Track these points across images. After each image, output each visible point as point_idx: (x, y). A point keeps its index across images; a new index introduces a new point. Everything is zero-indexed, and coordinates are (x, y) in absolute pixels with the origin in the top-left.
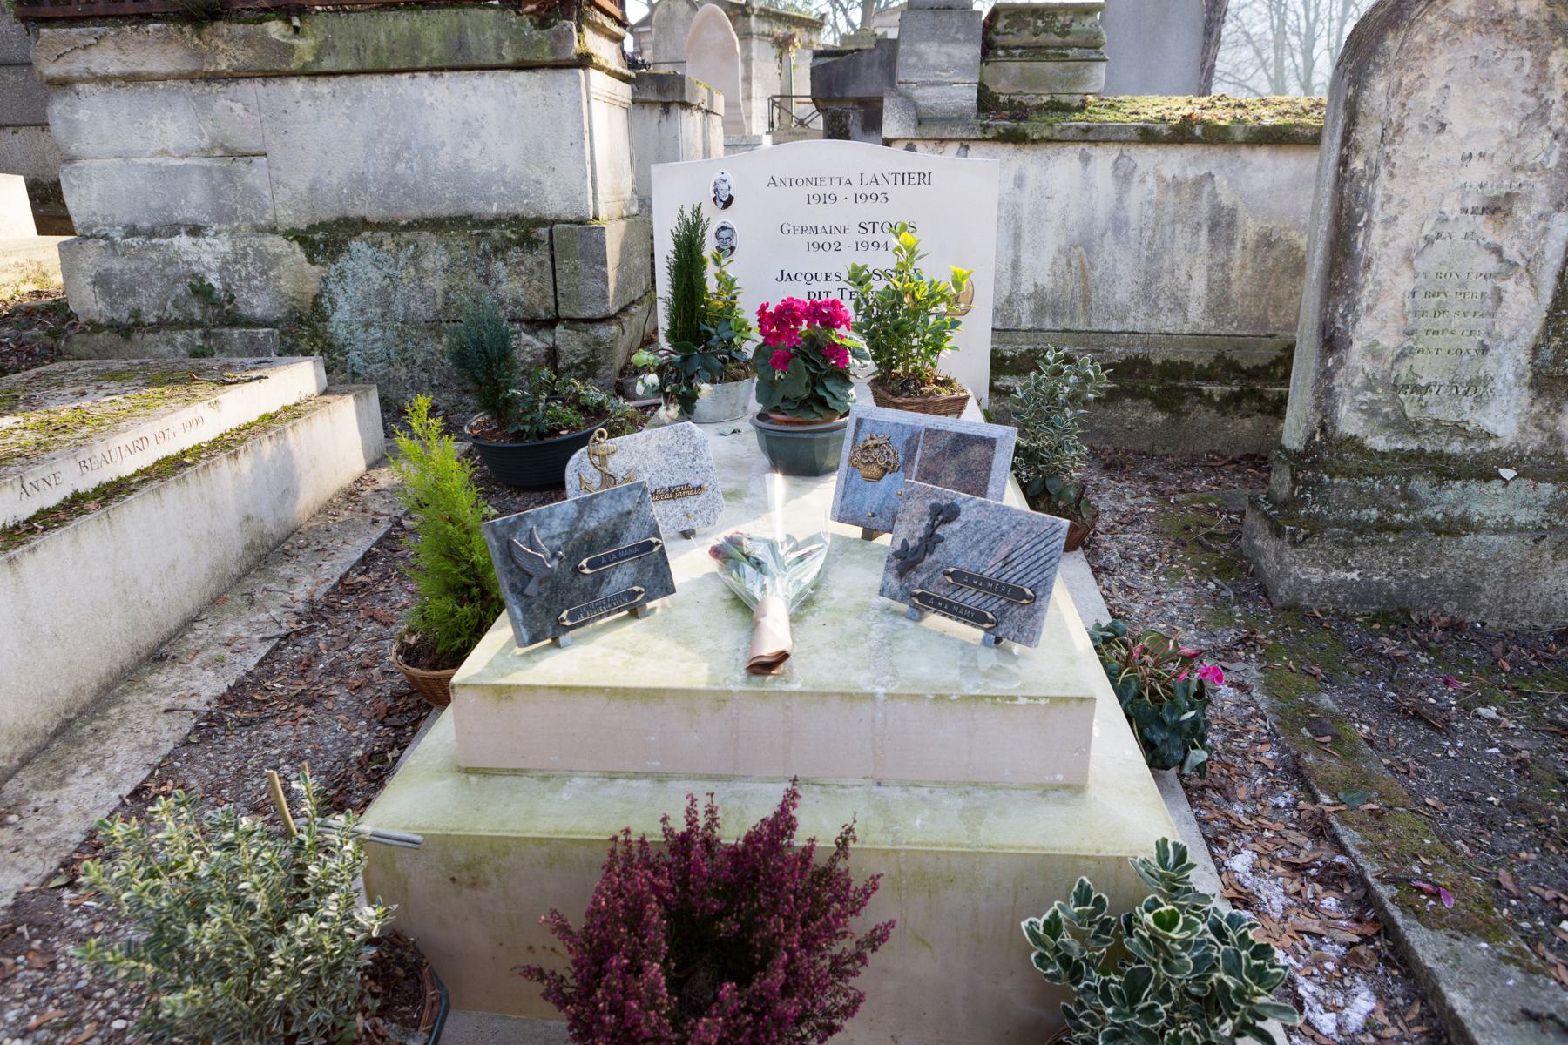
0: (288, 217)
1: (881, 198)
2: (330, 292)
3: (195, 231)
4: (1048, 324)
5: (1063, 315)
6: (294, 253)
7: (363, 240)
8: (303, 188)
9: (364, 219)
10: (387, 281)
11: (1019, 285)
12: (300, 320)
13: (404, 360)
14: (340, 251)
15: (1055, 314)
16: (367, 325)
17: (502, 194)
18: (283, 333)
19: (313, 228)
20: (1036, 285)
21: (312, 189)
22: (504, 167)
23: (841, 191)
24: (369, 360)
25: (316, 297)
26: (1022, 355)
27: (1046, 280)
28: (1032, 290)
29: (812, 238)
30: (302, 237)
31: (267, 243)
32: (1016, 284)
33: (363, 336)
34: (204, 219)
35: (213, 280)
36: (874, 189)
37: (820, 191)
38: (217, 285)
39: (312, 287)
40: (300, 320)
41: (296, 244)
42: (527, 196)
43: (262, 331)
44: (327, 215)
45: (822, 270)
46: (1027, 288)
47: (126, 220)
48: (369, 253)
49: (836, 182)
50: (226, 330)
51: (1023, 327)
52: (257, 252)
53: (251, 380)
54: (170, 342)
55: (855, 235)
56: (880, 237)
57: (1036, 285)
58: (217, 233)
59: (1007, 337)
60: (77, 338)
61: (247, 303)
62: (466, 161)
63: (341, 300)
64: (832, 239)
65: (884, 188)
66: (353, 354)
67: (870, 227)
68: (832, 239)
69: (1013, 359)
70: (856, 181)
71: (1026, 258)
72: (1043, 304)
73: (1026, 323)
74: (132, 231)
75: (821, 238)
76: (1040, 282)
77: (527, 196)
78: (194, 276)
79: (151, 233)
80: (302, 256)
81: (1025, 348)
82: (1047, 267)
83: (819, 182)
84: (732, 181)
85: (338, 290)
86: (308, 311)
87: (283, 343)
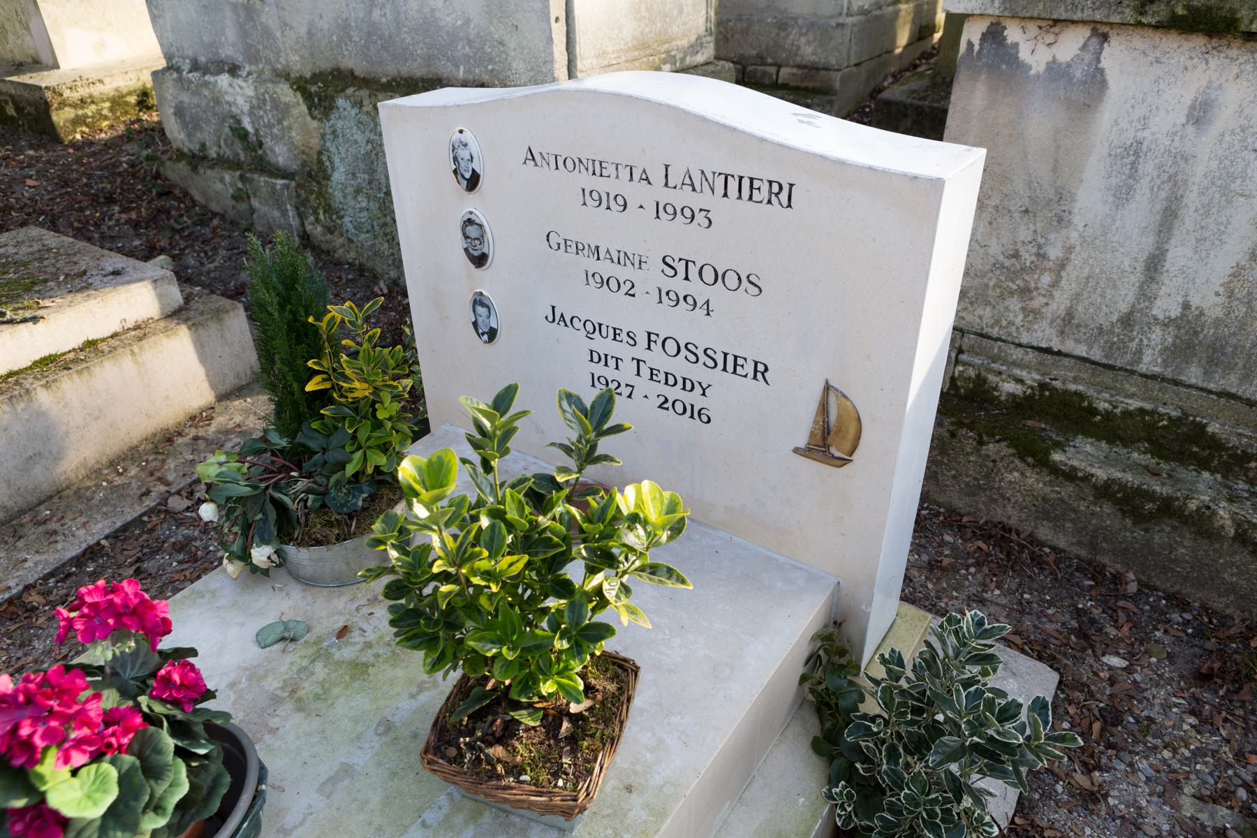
0: (297, 62)
1: (700, 217)
2: (328, 151)
3: (234, 70)
4: (1193, 374)
5: (1230, 367)
6: (298, 104)
7: (347, 98)
8: (303, 31)
9: (352, 72)
10: (370, 146)
11: (1152, 299)
12: (310, 175)
13: (386, 235)
14: (331, 108)
15: (1210, 361)
16: (358, 191)
17: (467, 55)
18: (299, 186)
19: (316, 77)
20: (1186, 306)
21: (310, 34)
22: (467, 21)
23: (635, 192)
24: (359, 228)
25: (320, 153)
26: (1127, 414)
27: (1208, 300)
28: (1175, 312)
29: (592, 265)
30: (301, 85)
31: (278, 90)
32: (1146, 293)
33: (352, 203)
34: (239, 58)
35: (247, 124)
36: (696, 201)
37: (602, 185)
38: (250, 128)
39: (315, 142)
40: (310, 175)
41: (299, 95)
42: (491, 60)
43: (280, 182)
44: (325, 66)
45: (610, 321)
46: (1167, 305)
47: (190, 53)
48: (353, 112)
49: (625, 173)
50: (256, 176)
51: (1143, 368)
52: (273, 100)
53: (24, 321)
54: (222, 180)
55: (652, 278)
56: (695, 288)
57: (1186, 306)
58: (249, 74)
59: (1107, 378)
60: (168, 164)
61: (272, 151)
62: (433, 10)
63: (337, 160)
64: (624, 273)
65: (703, 200)
66: (347, 219)
67: (680, 267)
68: (624, 273)
69: (1108, 416)
70: (657, 176)
71: (1179, 255)
72: (1189, 335)
73: (1150, 362)
74: (195, 66)
75: (606, 268)
76: (1195, 301)
77: (491, 60)
78: (234, 117)
79: (206, 71)
80: (304, 108)
81: (1134, 404)
82: (1217, 281)
83: (598, 169)
84: (474, 147)
85: (333, 149)
86: (315, 167)
87: (298, 196)
